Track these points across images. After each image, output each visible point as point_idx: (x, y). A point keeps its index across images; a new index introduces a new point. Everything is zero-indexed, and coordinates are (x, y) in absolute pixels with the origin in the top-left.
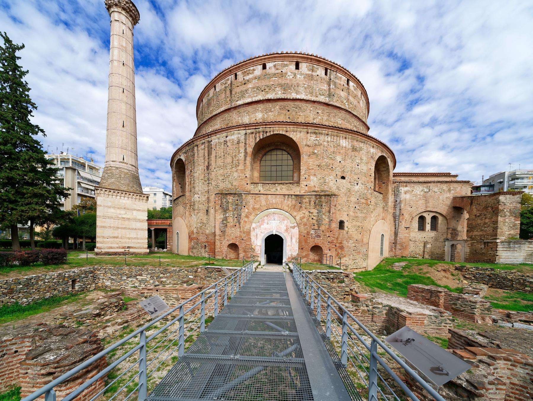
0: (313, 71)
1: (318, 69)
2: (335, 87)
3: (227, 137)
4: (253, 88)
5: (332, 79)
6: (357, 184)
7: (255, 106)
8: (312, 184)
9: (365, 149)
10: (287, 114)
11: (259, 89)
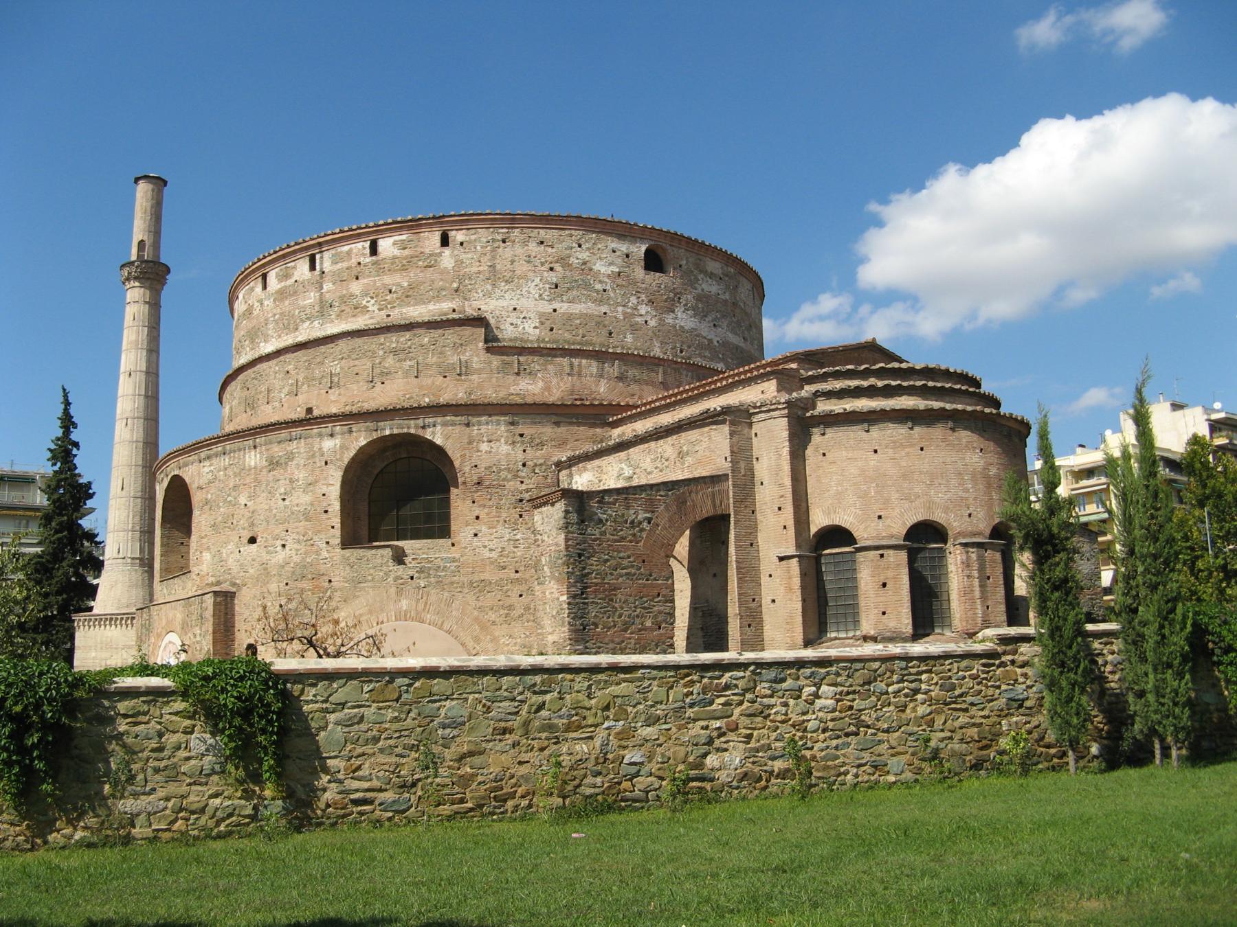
5: (326, 270)
6: (284, 546)
9: (302, 450)
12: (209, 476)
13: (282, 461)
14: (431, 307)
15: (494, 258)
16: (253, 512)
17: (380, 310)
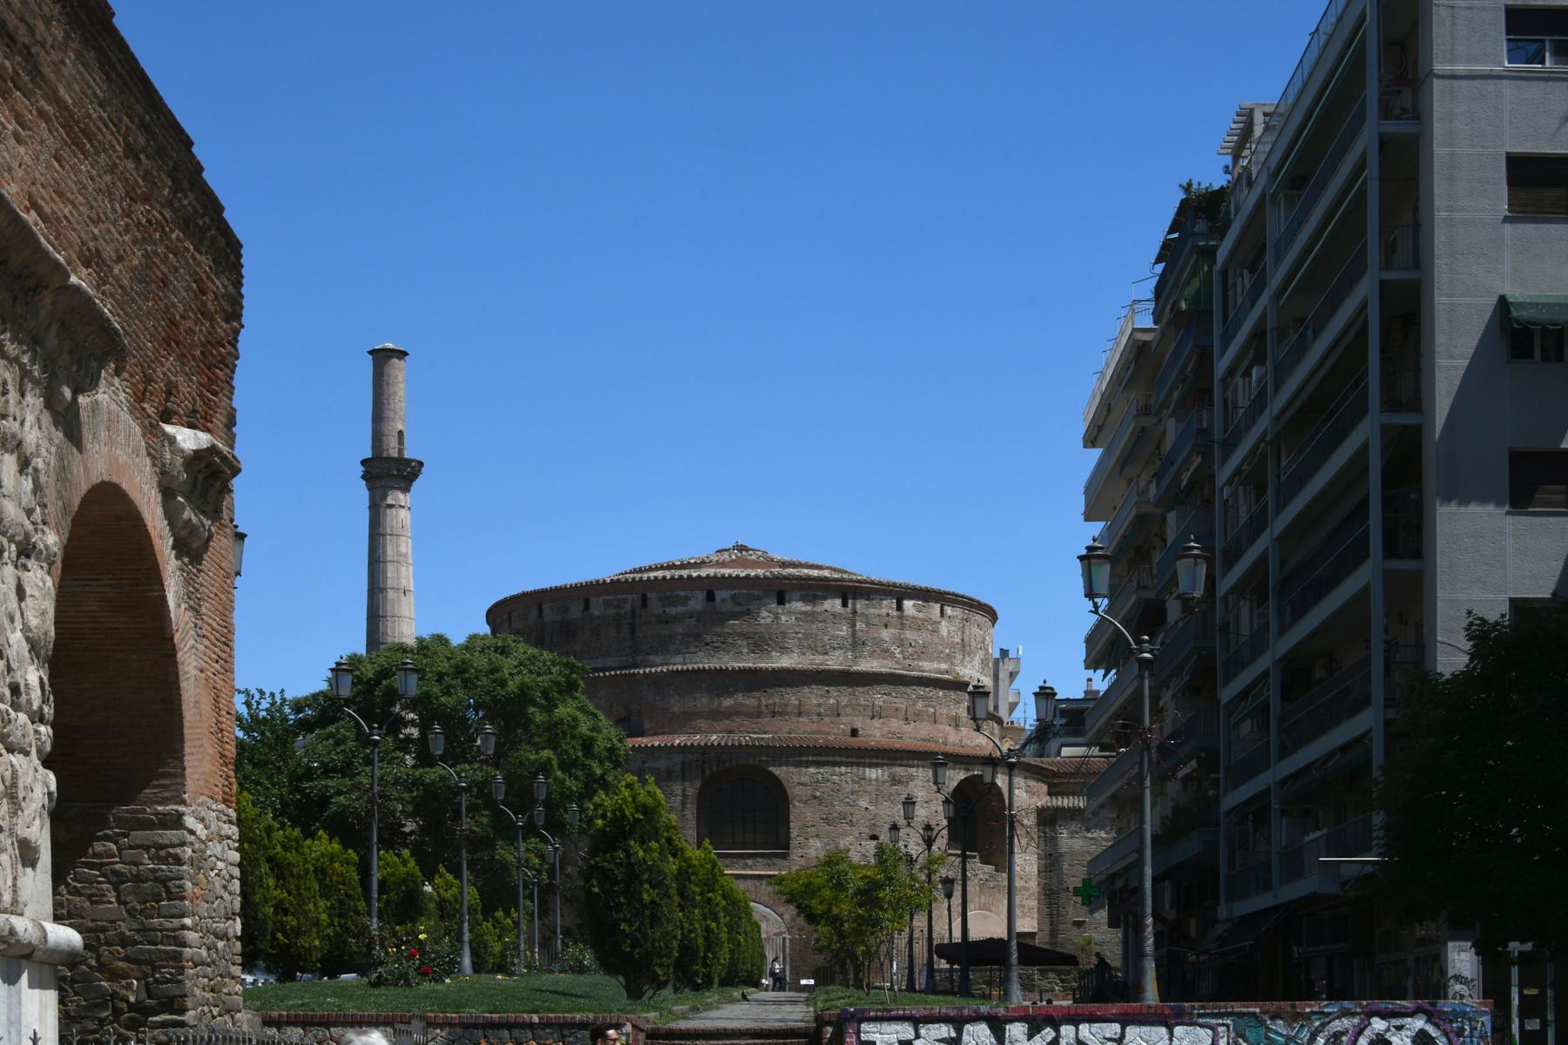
2: (868, 625)
3: (644, 763)
8: (812, 853)
10: (763, 698)
13: (904, 779)
15: (963, 632)
16: (876, 815)
17: (904, 659)
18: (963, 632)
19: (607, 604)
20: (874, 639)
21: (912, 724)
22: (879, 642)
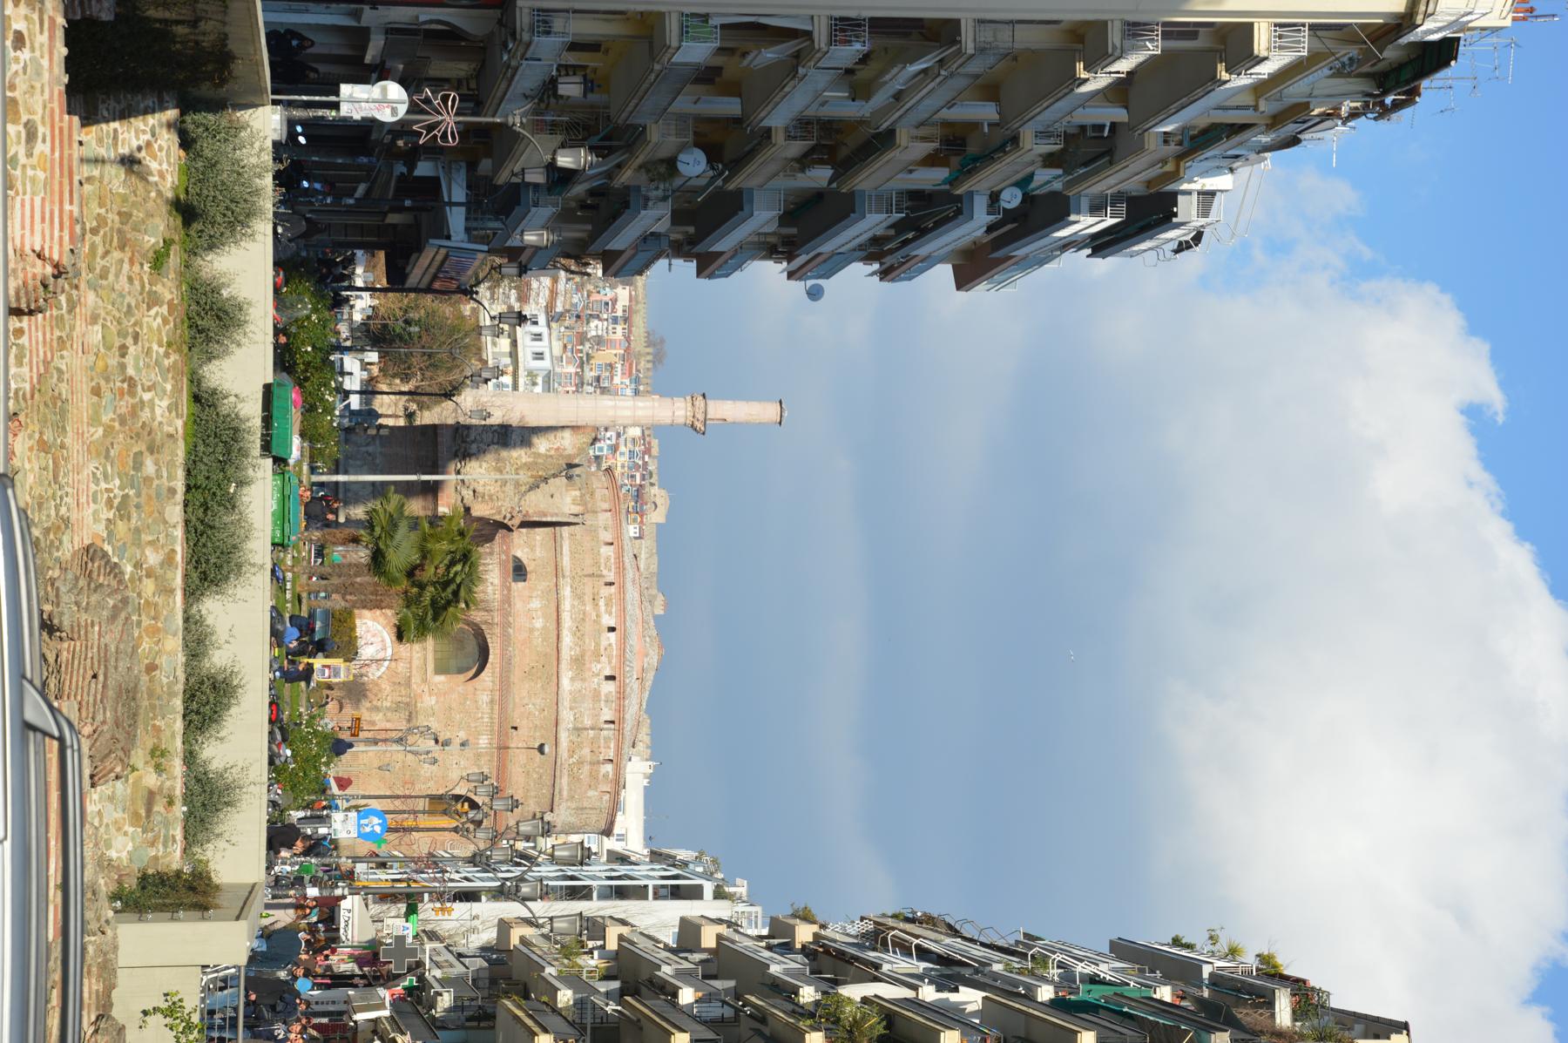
0: (606, 701)
1: (610, 709)
4: (584, 613)
7: (555, 617)
8: (426, 698)
11: (581, 620)
12: (480, 703)
14: (565, 788)
15: (591, 809)
18: (591, 809)
19: (608, 559)
20: (582, 743)
21: (521, 770)
22: (580, 746)
